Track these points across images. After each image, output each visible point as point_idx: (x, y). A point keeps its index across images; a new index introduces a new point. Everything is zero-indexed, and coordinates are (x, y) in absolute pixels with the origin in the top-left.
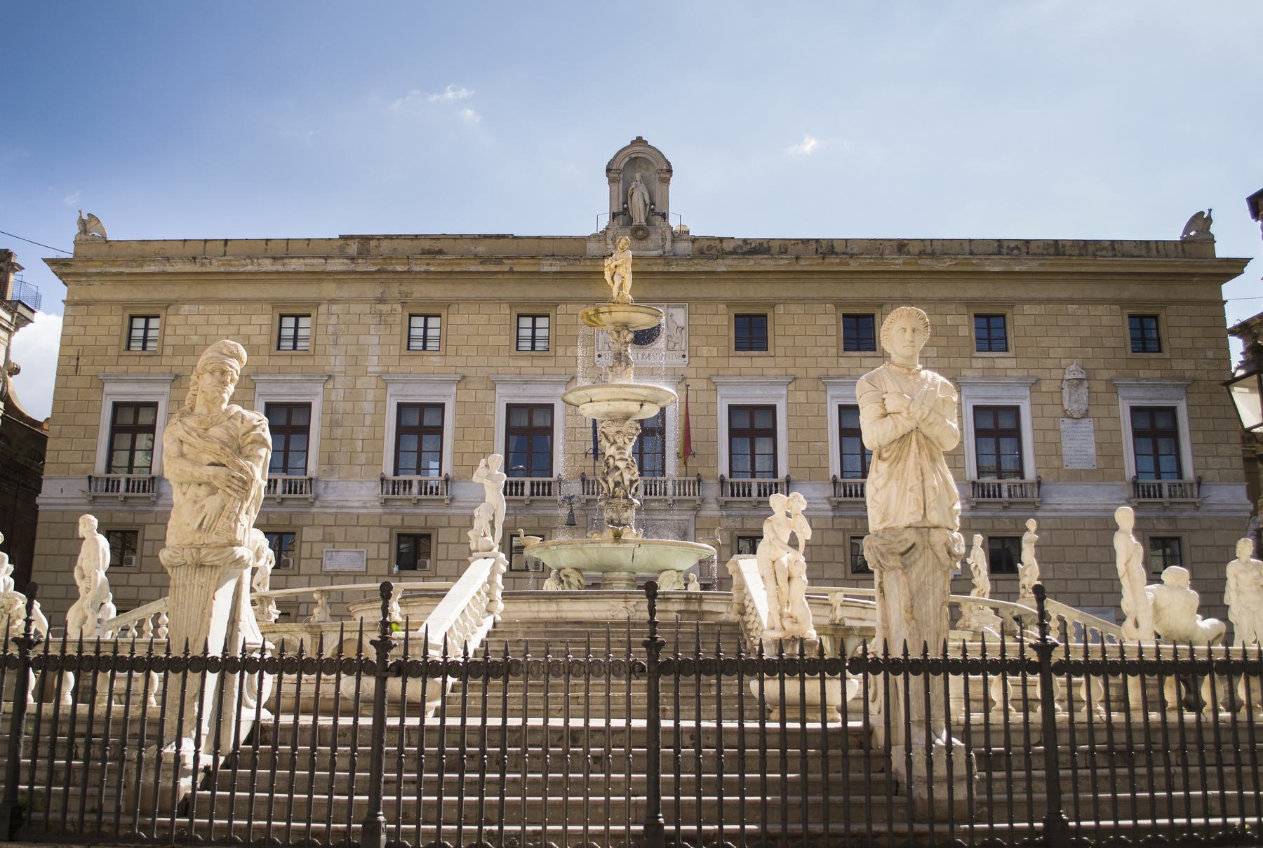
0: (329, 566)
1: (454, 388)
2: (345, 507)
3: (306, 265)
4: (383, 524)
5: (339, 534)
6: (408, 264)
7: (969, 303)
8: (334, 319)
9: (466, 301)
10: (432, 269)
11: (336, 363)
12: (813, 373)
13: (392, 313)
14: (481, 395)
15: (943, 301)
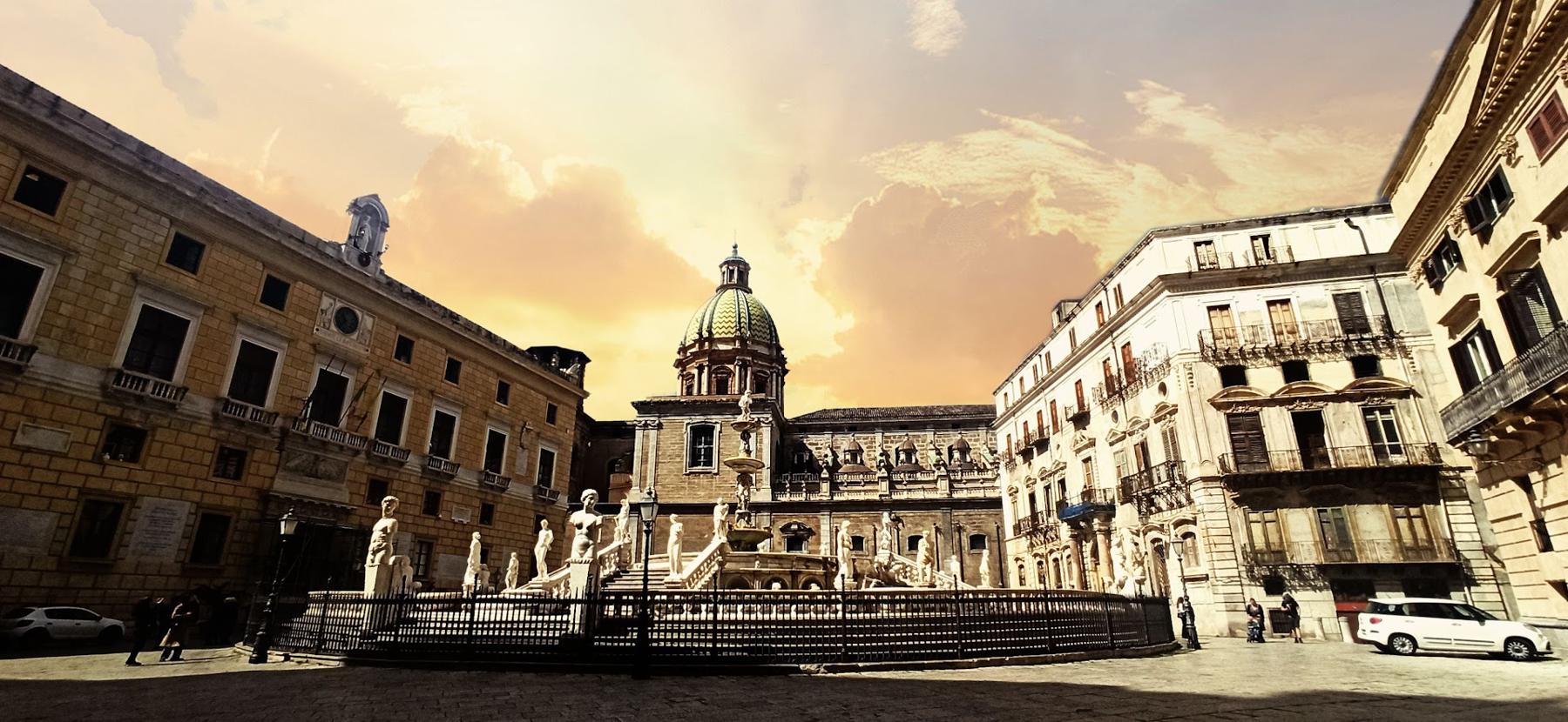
0: (20, 440)
1: (202, 313)
2: (58, 385)
3: (88, 137)
4: (99, 411)
5: (43, 410)
6: (199, 193)
7: (499, 374)
8: (92, 200)
9: (230, 245)
10: (218, 208)
11: (85, 239)
12: (429, 387)
13: (157, 223)
14: (224, 326)
15: (490, 368)
